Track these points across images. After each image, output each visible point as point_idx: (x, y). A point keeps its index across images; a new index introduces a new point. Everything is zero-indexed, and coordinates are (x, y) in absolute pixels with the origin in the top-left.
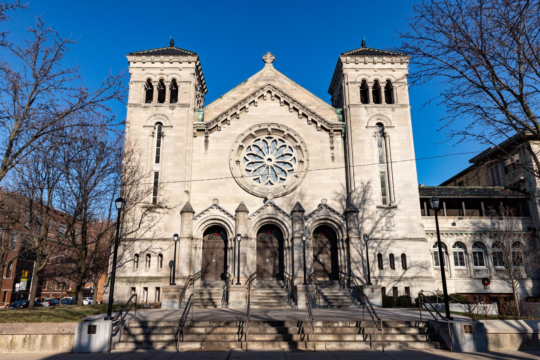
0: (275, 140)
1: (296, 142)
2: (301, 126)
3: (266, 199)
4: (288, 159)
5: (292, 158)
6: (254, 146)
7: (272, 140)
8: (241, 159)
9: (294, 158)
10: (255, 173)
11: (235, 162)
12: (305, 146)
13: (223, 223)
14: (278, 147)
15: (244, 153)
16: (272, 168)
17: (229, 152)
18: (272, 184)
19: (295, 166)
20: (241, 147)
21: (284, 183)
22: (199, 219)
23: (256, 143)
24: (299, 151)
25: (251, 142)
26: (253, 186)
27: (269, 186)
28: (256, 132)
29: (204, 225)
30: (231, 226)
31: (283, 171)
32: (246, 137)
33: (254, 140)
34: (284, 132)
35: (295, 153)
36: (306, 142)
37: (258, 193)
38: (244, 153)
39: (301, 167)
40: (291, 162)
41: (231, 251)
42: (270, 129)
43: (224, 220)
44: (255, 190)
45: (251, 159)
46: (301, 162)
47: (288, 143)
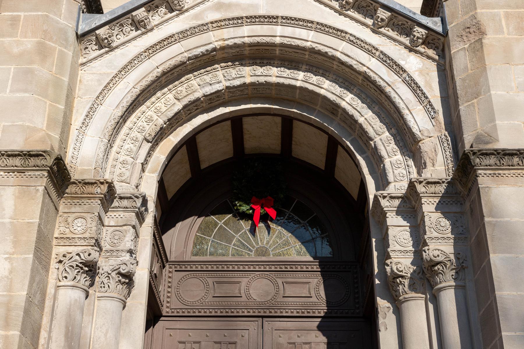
13: (327, 88)
22: (131, 45)
29: (167, 103)
30: (402, 95)
41: (417, 310)
43: (340, 49)
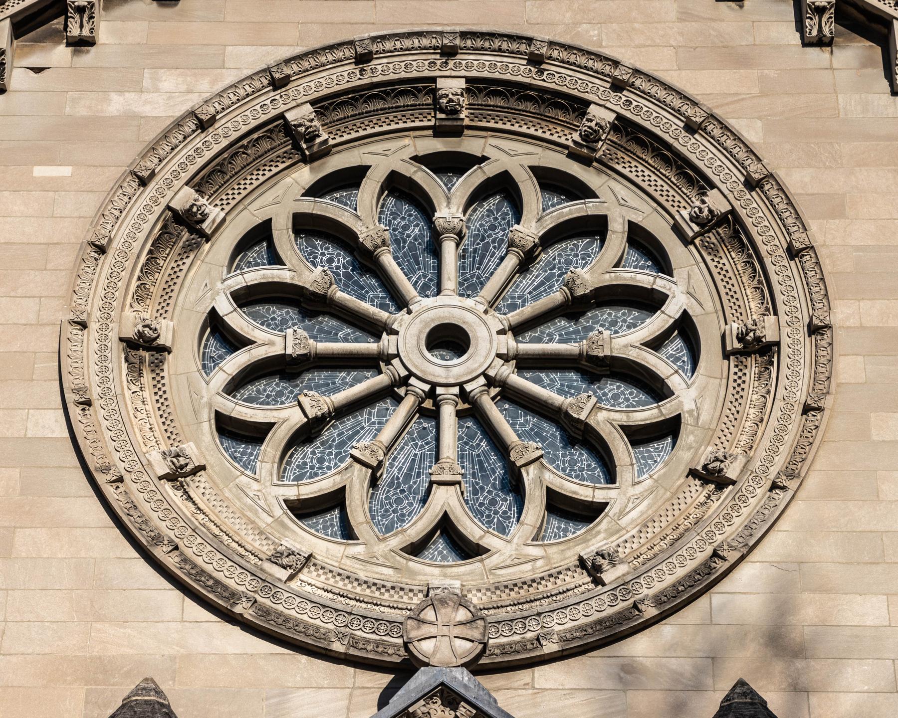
0: (503, 187)
1: (701, 182)
2: (738, 59)
3: (406, 667)
4: (625, 337)
5: (656, 324)
6: (307, 227)
7: (474, 178)
8: (180, 330)
9: (685, 327)
10: (306, 454)
11: (116, 352)
12: (788, 210)
14: (529, 230)
15: (209, 281)
16: (471, 411)
17: (66, 259)
18: (467, 550)
19: (694, 393)
20: (184, 228)
21: (594, 540)
23: (327, 207)
24: (731, 261)
25: (285, 194)
26: (276, 558)
27: (440, 572)
28: (324, 105)
31: (581, 436)
32: (236, 148)
33: (305, 176)
34: (578, 106)
35: (687, 287)
36: (796, 180)
37: (327, 624)
38: (209, 281)
39: (752, 394)
40: (657, 363)
42: (451, 86)
44: (301, 600)
45: (273, 337)
46: (756, 350)
47: (618, 199)
